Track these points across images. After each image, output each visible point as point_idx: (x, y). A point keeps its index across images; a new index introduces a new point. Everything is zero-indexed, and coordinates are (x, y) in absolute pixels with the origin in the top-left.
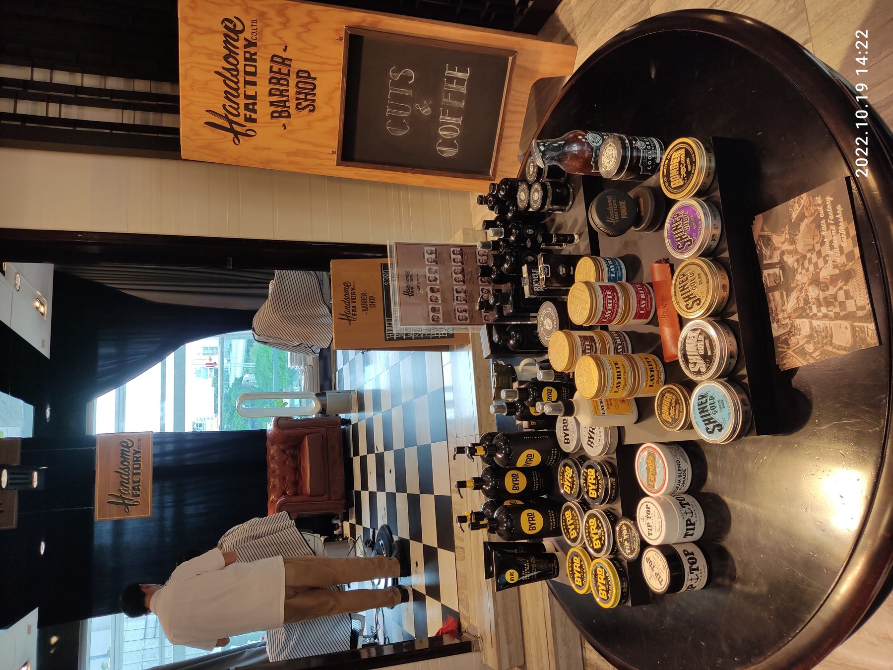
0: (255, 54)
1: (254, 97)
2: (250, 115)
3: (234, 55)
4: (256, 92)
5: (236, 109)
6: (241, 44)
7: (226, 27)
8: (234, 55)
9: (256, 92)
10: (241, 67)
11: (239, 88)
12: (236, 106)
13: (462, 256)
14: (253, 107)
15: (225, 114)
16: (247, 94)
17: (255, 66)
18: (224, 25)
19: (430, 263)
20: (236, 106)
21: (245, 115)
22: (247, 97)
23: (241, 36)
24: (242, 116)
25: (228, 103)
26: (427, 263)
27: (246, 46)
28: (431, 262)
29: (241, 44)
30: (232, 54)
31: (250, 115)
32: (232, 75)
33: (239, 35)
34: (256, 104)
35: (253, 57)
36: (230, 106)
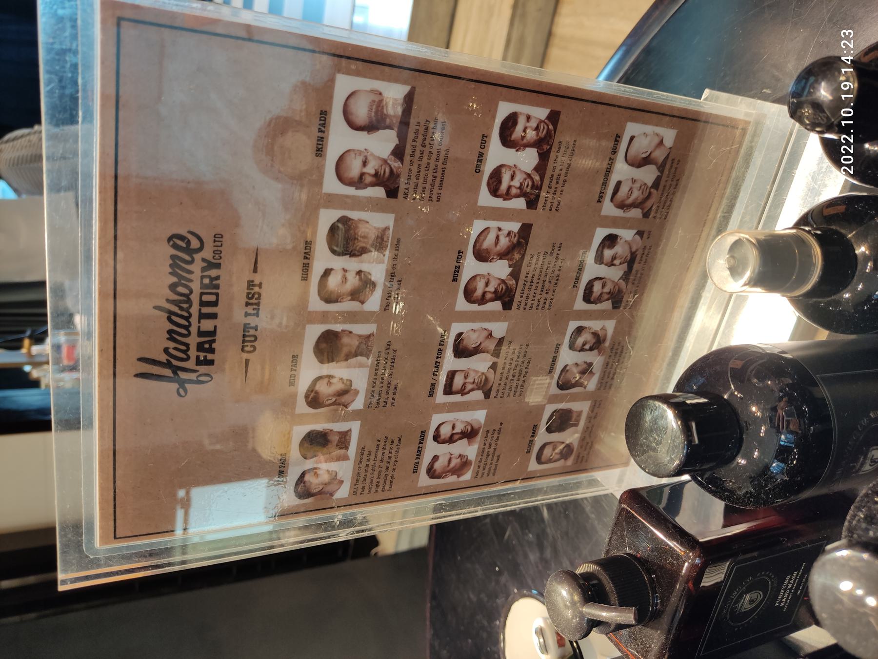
0: (218, 278)
1: (213, 333)
2: (205, 357)
3: (187, 283)
4: (215, 327)
5: (185, 352)
6: (197, 267)
7: (175, 246)
8: (187, 283)
9: (215, 327)
10: (195, 298)
11: (190, 325)
12: (184, 348)
13: (544, 157)
14: (211, 345)
15: (167, 360)
16: (201, 330)
17: (217, 295)
18: (171, 243)
19: (351, 191)
20: (184, 348)
21: (198, 357)
22: (201, 334)
23: (198, 257)
24: (193, 359)
25: (171, 345)
26: (331, 185)
27: (204, 269)
28: (359, 182)
29: (197, 267)
30: (182, 281)
31: (205, 357)
32: (181, 308)
33: (194, 256)
34: (214, 341)
35: (214, 282)
36: (176, 349)
